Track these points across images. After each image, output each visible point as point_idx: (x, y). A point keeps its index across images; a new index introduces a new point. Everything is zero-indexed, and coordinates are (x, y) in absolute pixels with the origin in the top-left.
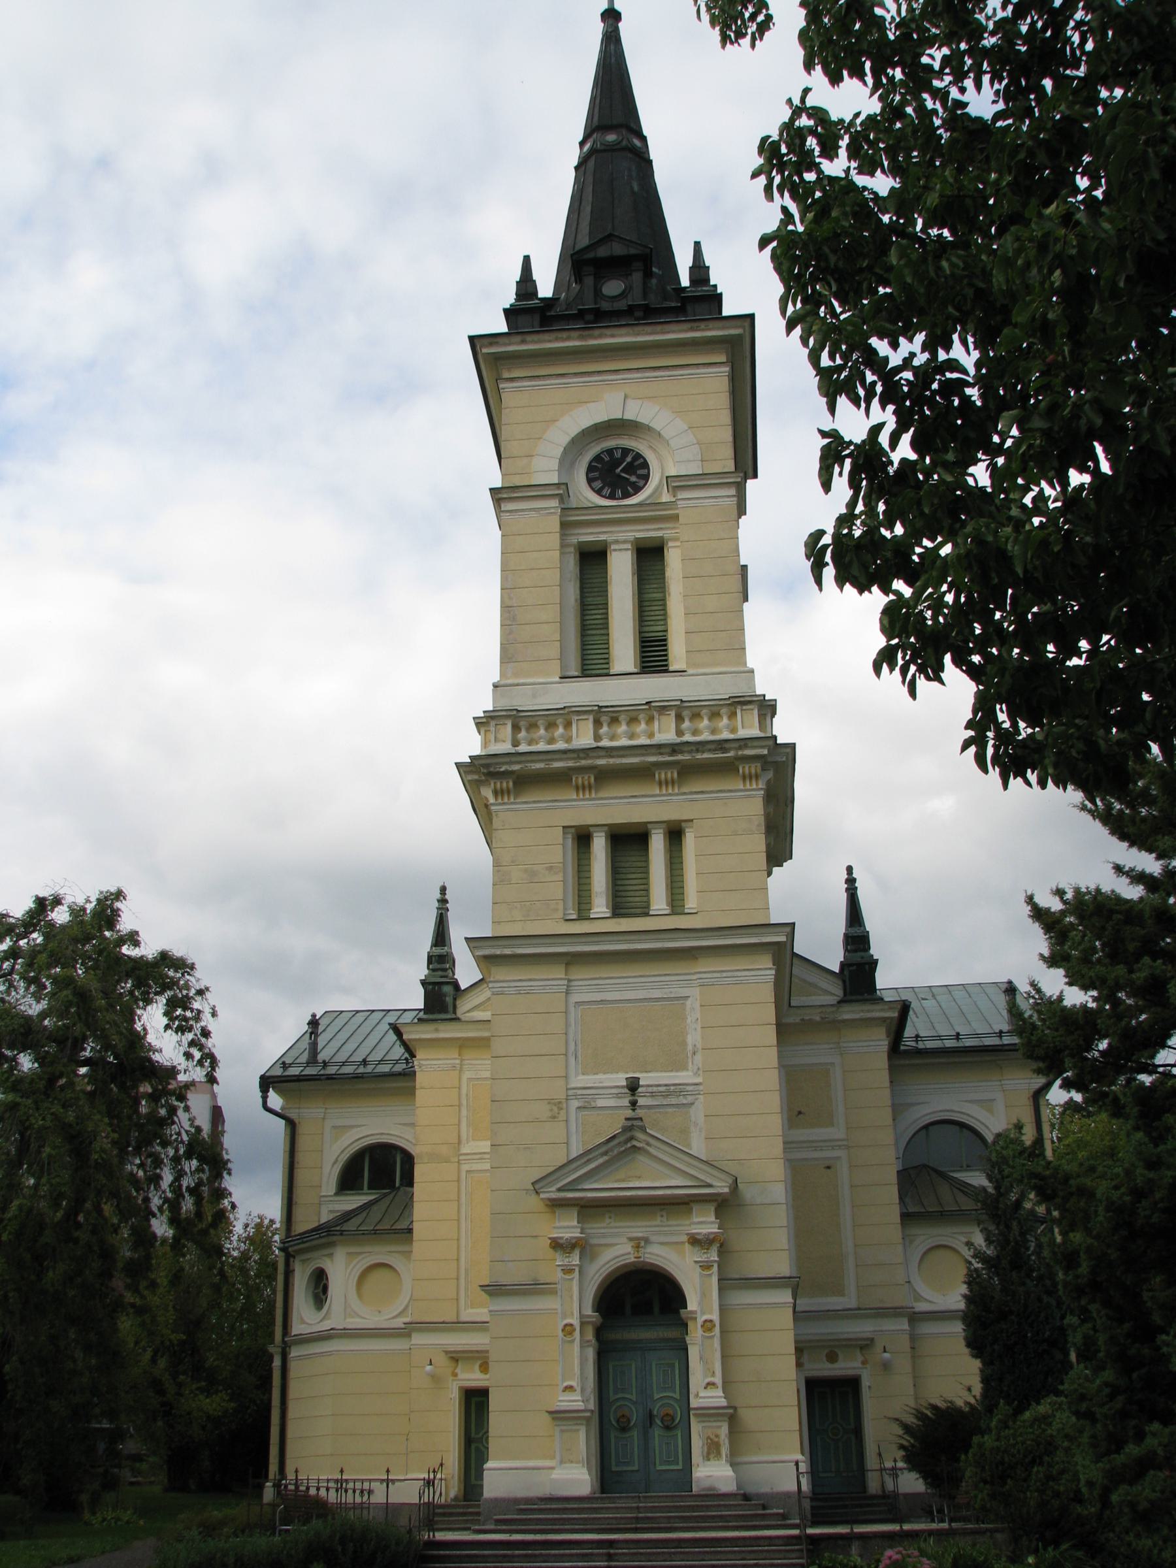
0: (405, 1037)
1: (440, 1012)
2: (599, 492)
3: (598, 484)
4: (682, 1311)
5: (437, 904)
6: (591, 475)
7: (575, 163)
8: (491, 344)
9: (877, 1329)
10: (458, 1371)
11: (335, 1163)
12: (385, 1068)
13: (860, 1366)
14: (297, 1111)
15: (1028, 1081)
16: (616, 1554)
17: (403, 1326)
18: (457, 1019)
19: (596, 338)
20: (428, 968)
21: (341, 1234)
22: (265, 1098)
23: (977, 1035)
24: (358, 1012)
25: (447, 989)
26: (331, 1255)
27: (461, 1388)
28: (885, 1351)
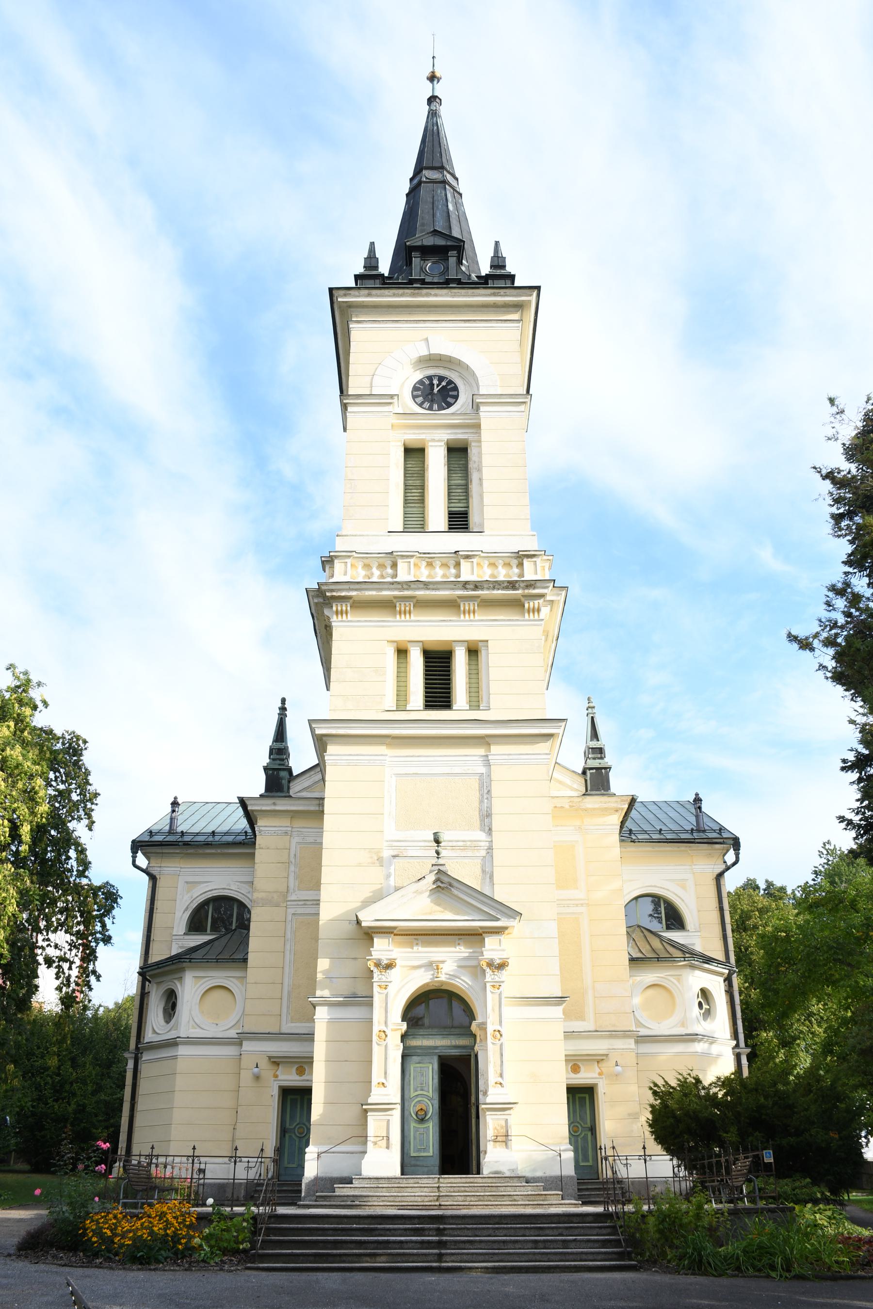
1: (277, 792)
3: (420, 400)
5: (278, 711)
6: (415, 393)
8: (345, 295)
9: (611, 1047)
10: (278, 1073)
11: (187, 908)
12: (230, 839)
13: (598, 1076)
14: (159, 869)
15: (712, 866)
16: (445, 1229)
17: (236, 1036)
18: (290, 797)
19: (423, 296)
20: (270, 758)
21: (190, 962)
22: (134, 858)
23: (673, 832)
24: (207, 803)
25: (284, 774)
26: (180, 979)
27: (280, 1087)
28: (617, 1065)
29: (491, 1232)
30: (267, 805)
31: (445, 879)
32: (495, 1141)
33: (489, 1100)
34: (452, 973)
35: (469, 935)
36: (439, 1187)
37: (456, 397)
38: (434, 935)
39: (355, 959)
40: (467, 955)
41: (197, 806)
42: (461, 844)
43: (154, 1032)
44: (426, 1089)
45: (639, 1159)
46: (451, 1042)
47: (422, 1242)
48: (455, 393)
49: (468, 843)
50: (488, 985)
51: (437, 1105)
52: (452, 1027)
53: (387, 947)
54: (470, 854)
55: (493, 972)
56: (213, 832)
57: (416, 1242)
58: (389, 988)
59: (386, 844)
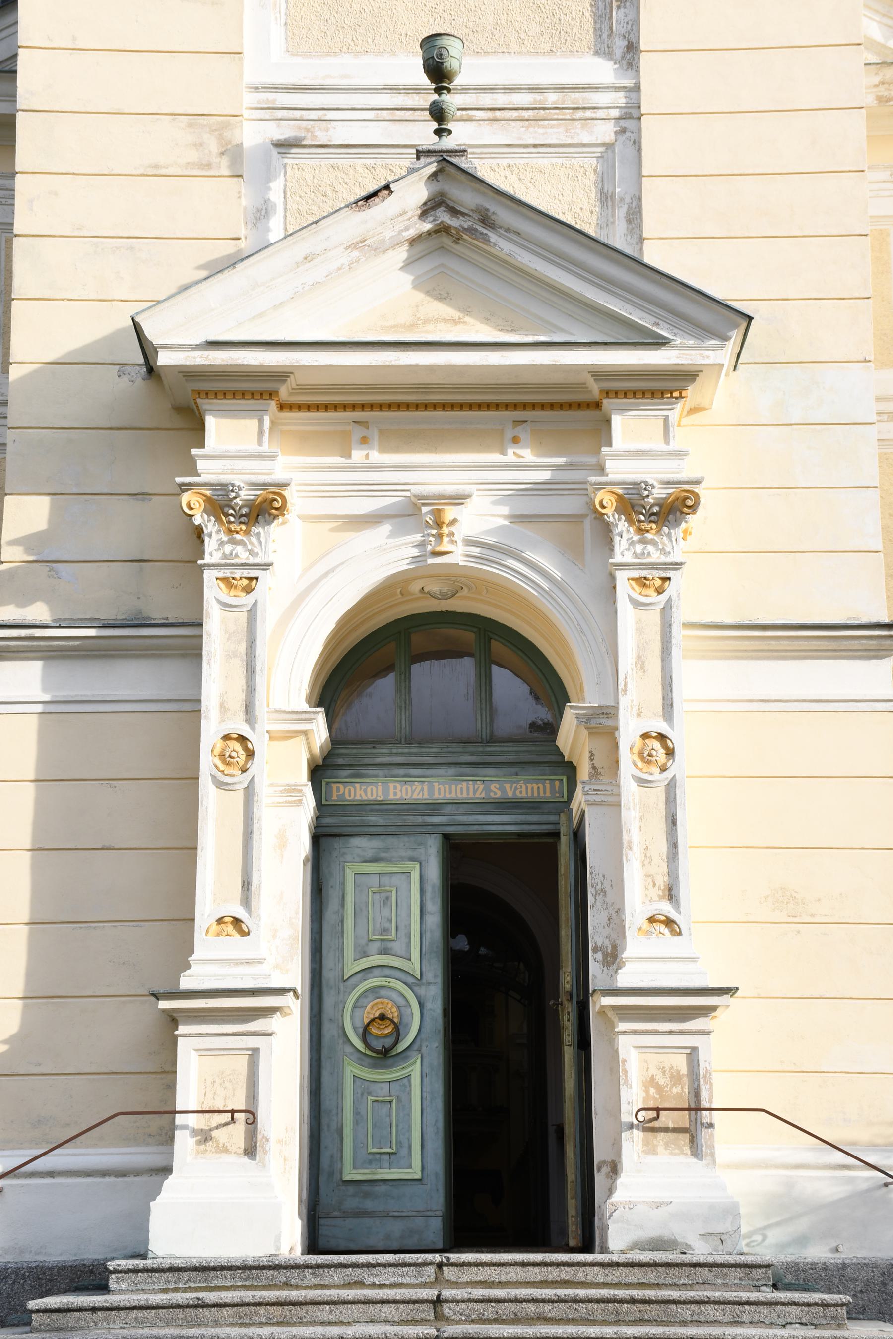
31: (466, 198)
32: (650, 1128)
33: (625, 978)
34: (490, 539)
35: (552, 406)
36: (438, 1302)
38: (426, 406)
39: (142, 496)
40: (545, 475)
44: (397, 947)
46: (487, 790)
49: (552, 98)
50: (622, 577)
51: (436, 1006)
52: (492, 740)
53: (252, 446)
55: (640, 531)
58: (260, 588)
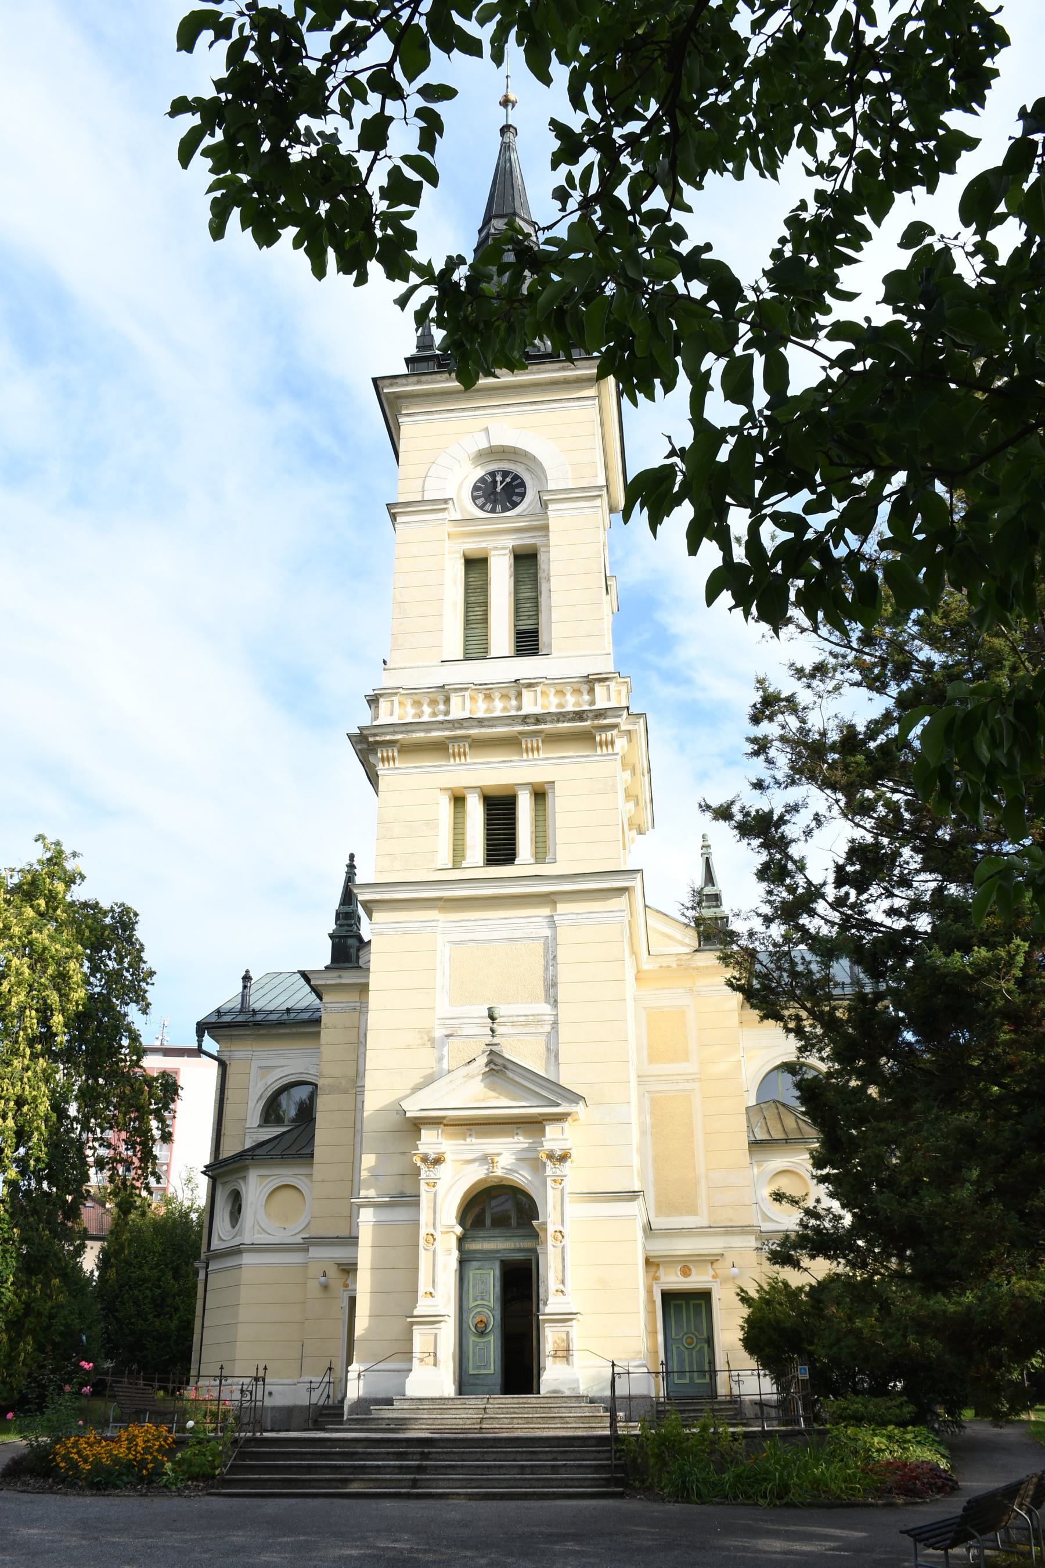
0: (312, 983)
1: (344, 962)
2: (482, 508)
4: (534, 1223)
5: (346, 869)
7: (475, 246)
8: (391, 385)
11: (259, 1099)
16: (429, 1453)
17: (301, 1241)
25: (351, 942)
26: (244, 1178)
29: (478, 1456)
30: (332, 979)
31: (499, 1061)
32: (555, 1357)
33: (548, 1309)
36: (485, 1409)
37: (523, 495)
38: (489, 1124)
40: (526, 1145)
41: (282, 977)
42: (522, 1019)
43: (220, 1239)
44: (486, 1298)
45: (753, 1375)
47: (401, 1467)
48: (521, 490)
49: (531, 1018)
50: (549, 1179)
51: (498, 1317)
53: (435, 1140)
54: (532, 1030)
56: (288, 1009)
57: (394, 1467)
58: (437, 1186)
59: (437, 1022)
